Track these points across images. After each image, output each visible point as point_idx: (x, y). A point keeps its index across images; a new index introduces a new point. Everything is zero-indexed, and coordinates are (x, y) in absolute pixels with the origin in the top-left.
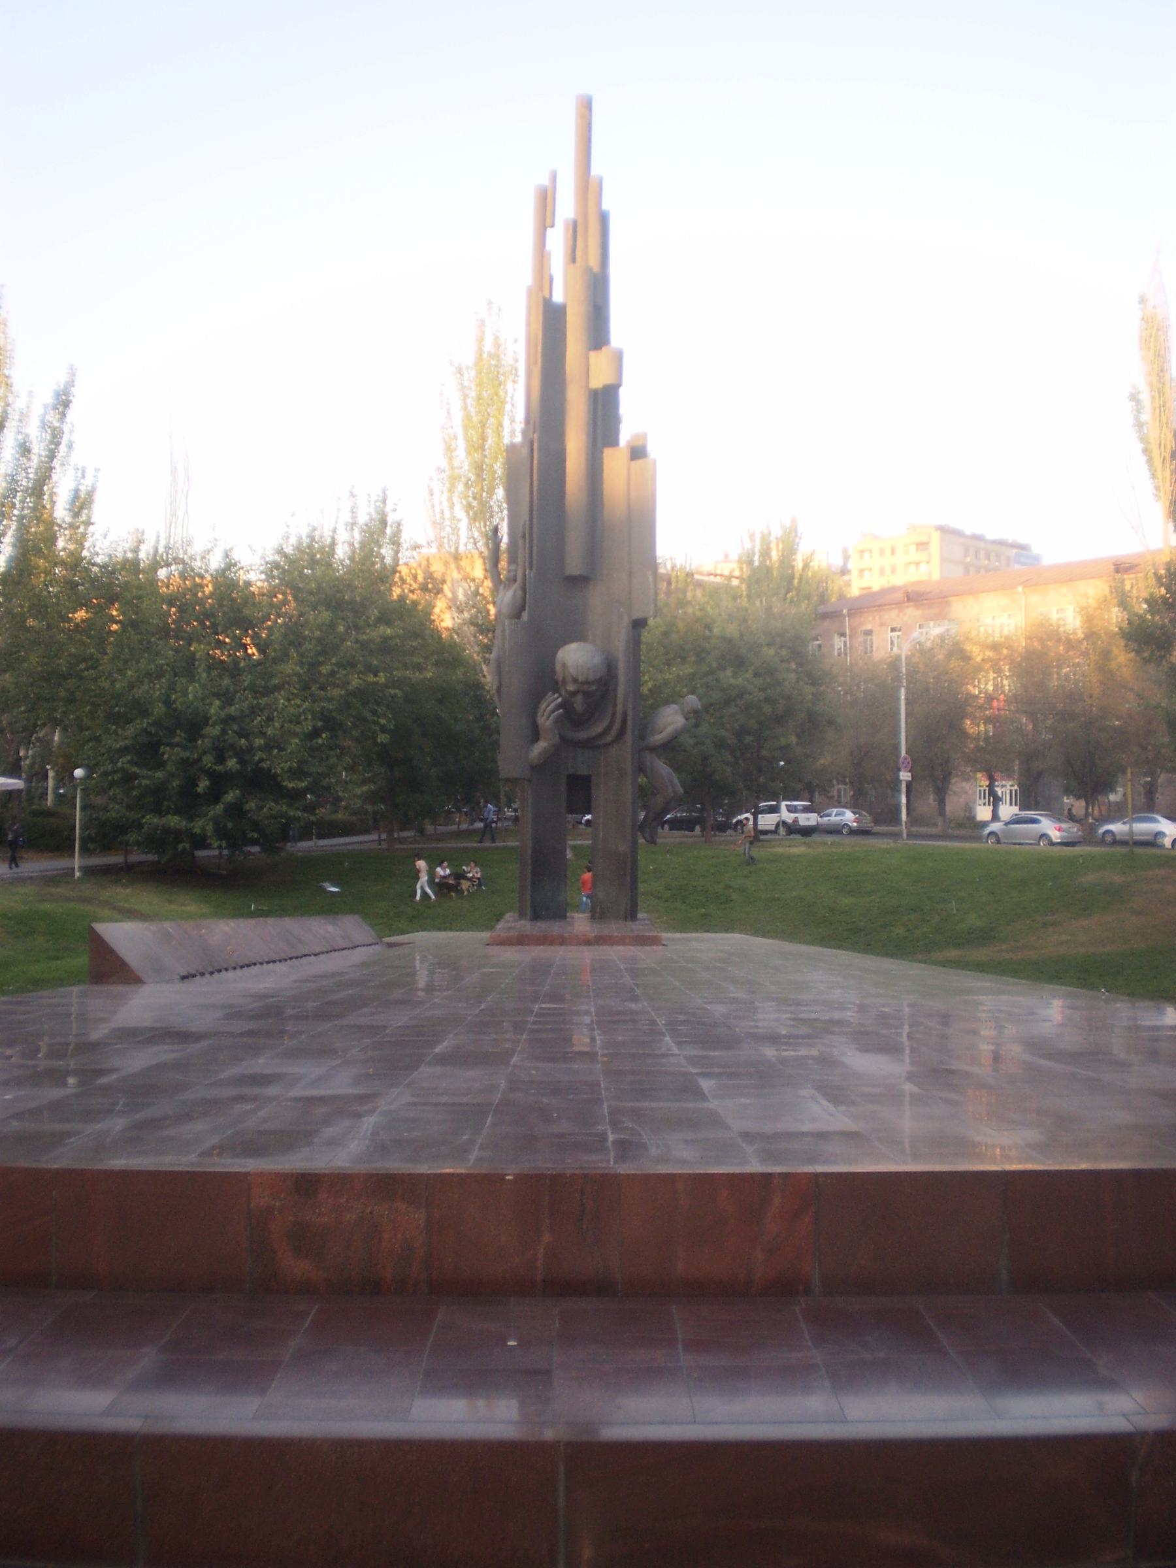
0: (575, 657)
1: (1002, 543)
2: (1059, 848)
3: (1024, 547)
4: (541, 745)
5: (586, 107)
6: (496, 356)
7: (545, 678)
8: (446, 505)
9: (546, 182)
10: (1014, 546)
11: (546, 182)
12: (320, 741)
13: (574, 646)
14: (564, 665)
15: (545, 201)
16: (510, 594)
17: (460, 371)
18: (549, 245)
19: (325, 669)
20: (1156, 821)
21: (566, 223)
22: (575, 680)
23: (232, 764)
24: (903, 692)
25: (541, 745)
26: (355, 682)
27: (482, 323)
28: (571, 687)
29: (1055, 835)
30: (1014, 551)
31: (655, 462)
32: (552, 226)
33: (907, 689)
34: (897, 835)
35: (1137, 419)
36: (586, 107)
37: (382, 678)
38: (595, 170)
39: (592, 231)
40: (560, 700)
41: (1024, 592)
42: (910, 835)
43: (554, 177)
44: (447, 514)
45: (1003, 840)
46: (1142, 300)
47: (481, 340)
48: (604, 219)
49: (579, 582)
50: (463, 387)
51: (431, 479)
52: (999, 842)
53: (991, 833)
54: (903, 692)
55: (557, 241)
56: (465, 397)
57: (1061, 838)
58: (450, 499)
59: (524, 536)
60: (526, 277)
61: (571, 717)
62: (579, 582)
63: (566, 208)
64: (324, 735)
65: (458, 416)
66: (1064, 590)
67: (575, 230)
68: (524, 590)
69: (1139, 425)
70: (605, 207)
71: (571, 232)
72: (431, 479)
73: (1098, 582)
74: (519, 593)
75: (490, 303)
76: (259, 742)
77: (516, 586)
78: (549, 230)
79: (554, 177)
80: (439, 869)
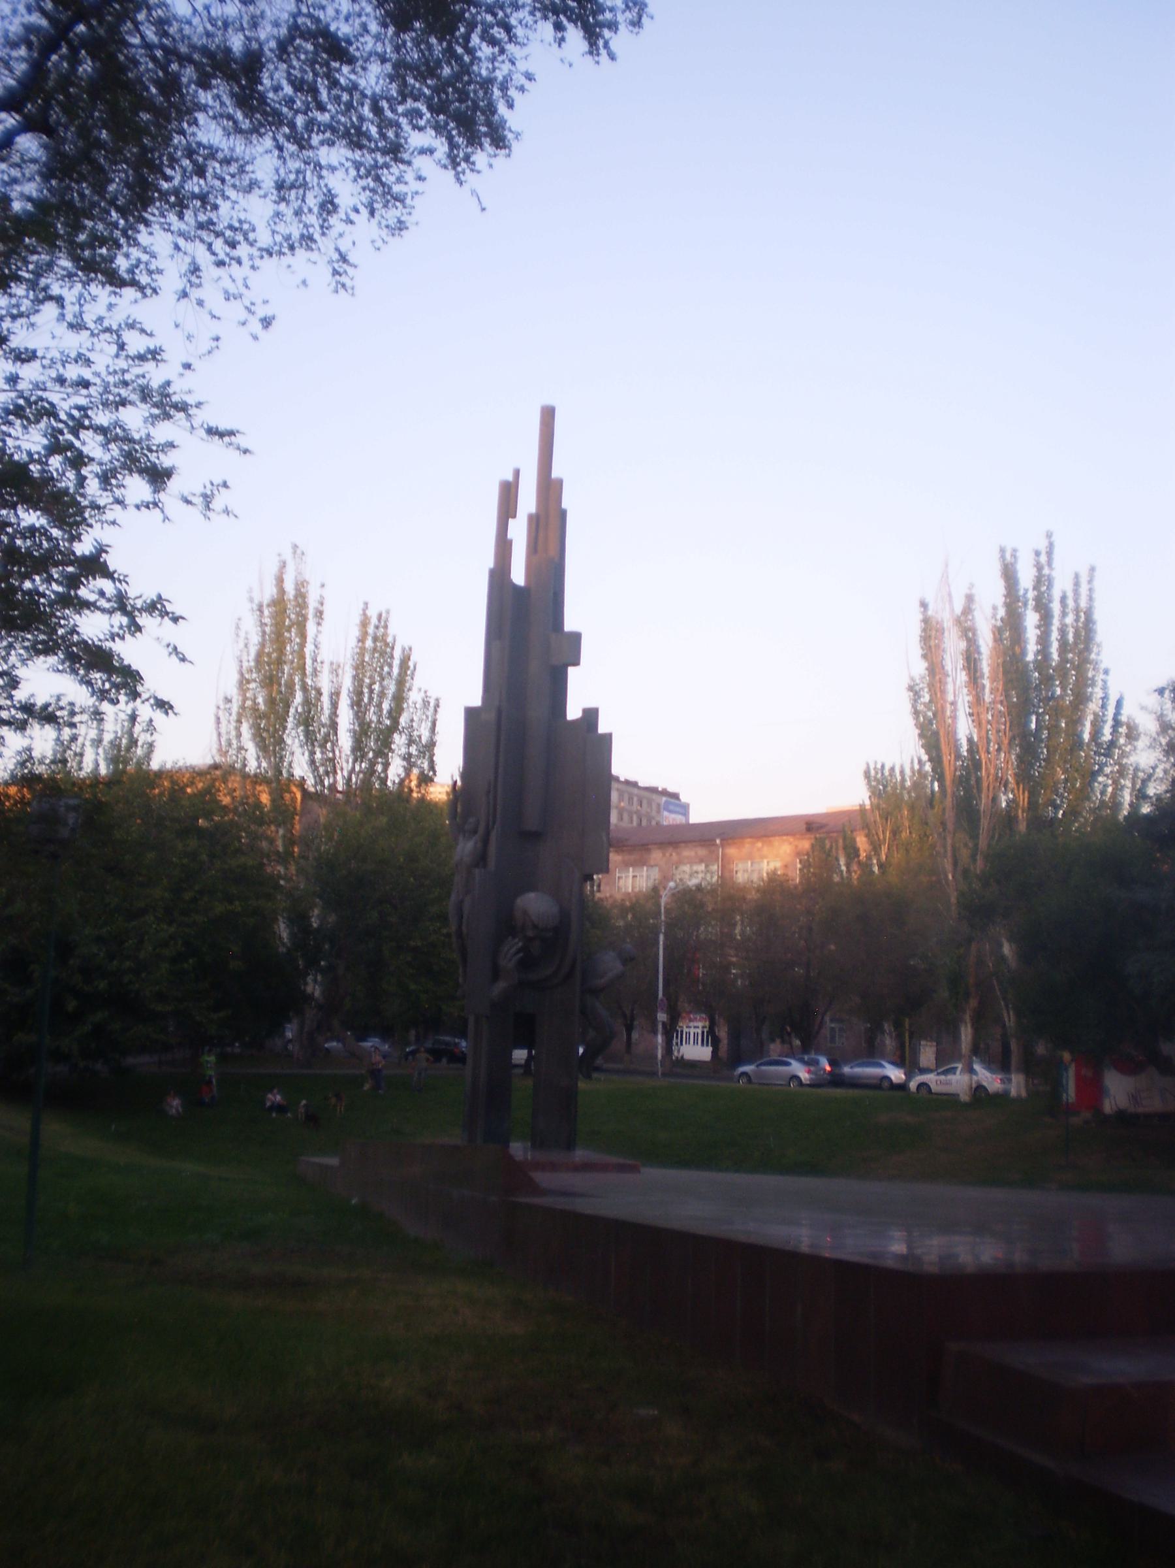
0: (535, 904)
1: (653, 790)
2: (808, 1090)
3: (675, 796)
4: (501, 985)
5: (548, 416)
6: (301, 596)
7: (508, 924)
8: (233, 733)
9: (510, 478)
10: (665, 793)
11: (510, 478)
12: (186, 966)
13: (532, 895)
14: (525, 913)
15: (508, 494)
16: (470, 845)
17: (260, 609)
18: (511, 535)
19: (188, 896)
20: (882, 1066)
21: (530, 517)
22: (535, 927)
23: (102, 985)
24: (661, 937)
25: (501, 985)
26: (219, 908)
27: (283, 565)
28: (530, 933)
29: (804, 1076)
30: (664, 799)
31: (610, 735)
32: (514, 516)
33: (666, 935)
34: (654, 1074)
35: (914, 707)
36: (548, 416)
37: (237, 906)
39: (550, 525)
40: (520, 944)
41: (722, 845)
42: (664, 1074)
43: (517, 473)
44: (234, 742)
45: (754, 1080)
46: (924, 605)
47: (280, 581)
48: (563, 514)
49: (533, 837)
50: (263, 625)
51: (218, 708)
52: (750, 1081)
53: (744, 1074)
54: (661, 937)
55: (518, 531)
56: (264, 633)
57: (811, 1079)
58: (238, 729)
59: (489, 792)
60: (488, 561)
61: (527, 962)
62: (533, 837)
63: (527, 502)
64: (191, 961)
65: (253, 650)
66: (759, 845)
67: (537, 523)
68: (486, 841)
69: (916, 713)
70: (564, 506)
71: (534, 526)
72: (218, 708)
74: (479, 845)
75: (295, 547)
76: (128, 964)
79: (517, 473)
80: (270, 1096)
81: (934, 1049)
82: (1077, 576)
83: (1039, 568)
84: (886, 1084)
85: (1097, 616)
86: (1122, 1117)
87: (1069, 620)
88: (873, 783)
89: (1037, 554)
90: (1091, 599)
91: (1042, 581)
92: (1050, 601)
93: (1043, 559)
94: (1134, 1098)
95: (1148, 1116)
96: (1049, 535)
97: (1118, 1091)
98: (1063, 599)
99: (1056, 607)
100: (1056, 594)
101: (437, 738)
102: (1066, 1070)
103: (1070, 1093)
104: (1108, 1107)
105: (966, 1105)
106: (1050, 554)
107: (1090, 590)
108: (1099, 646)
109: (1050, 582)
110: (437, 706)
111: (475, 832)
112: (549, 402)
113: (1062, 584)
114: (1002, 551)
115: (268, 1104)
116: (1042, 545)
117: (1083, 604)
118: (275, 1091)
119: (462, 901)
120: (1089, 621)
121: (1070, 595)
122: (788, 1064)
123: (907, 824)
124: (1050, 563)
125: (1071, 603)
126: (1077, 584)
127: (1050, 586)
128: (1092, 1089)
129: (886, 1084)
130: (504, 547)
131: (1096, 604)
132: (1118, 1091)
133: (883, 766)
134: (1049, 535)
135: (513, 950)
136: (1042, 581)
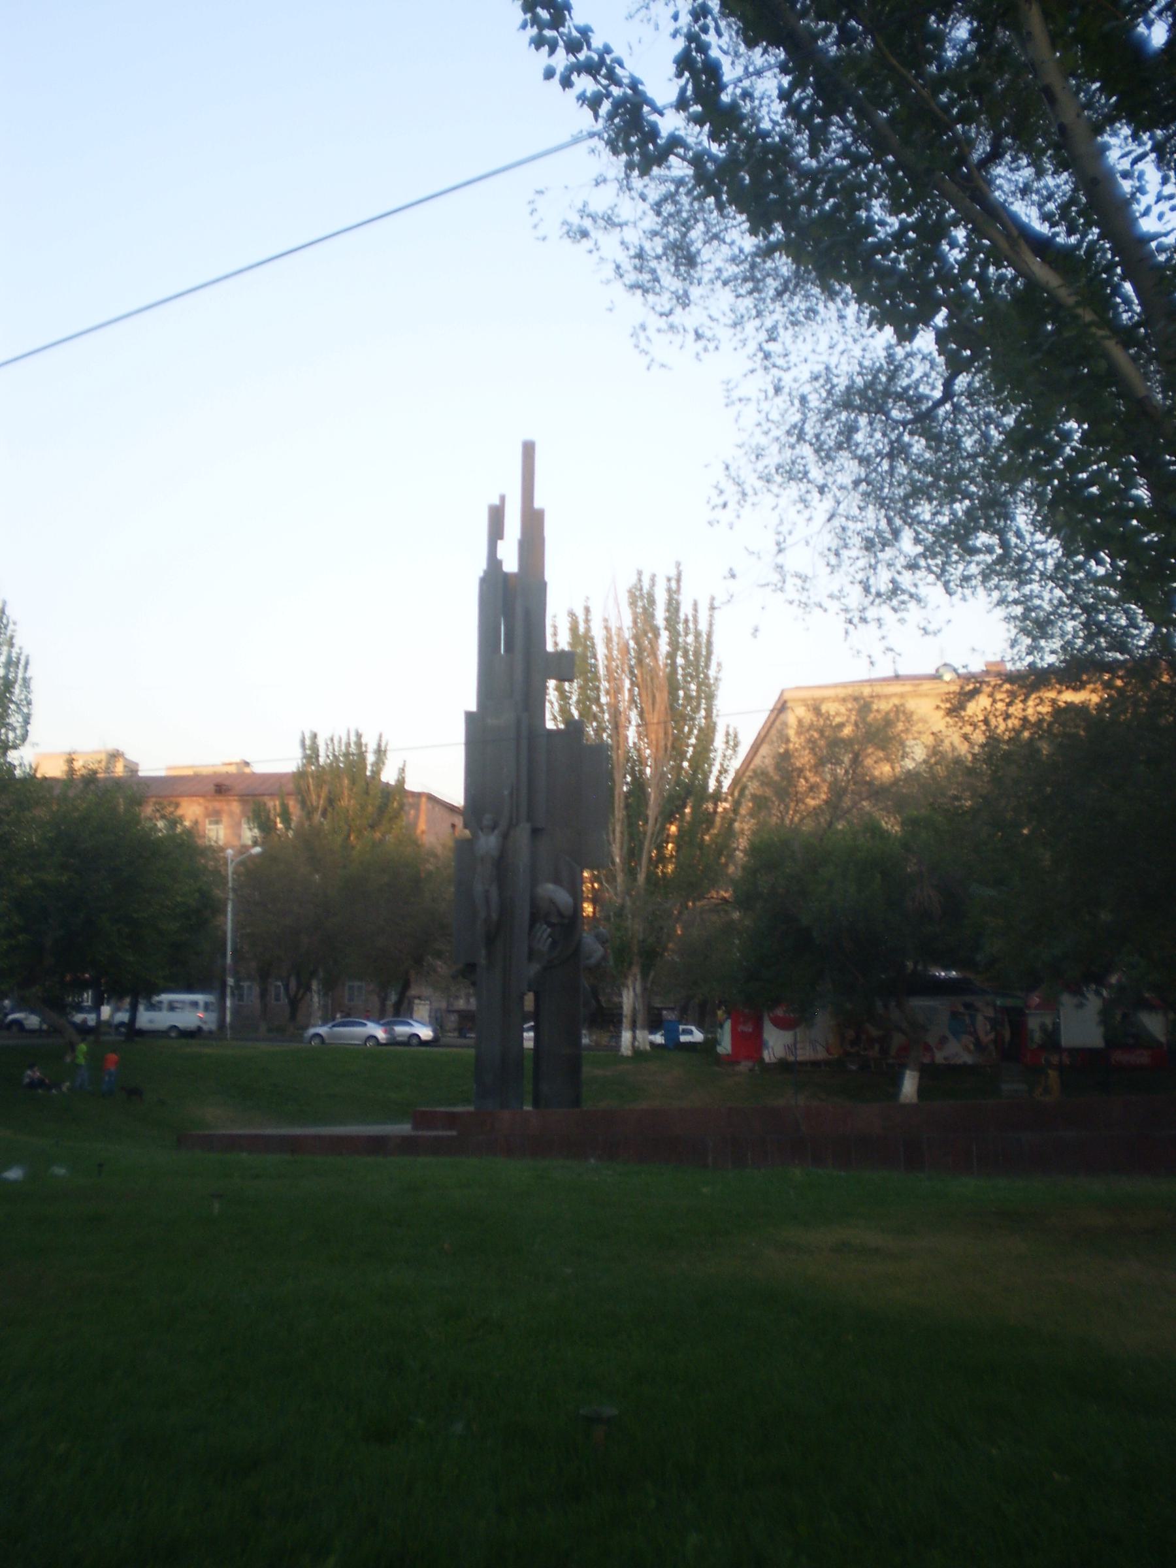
5: (529, 450)
11: (497, 502)
14: (552, 902)
15: (496, 516)
22: (560, 915)
25: (534, 968)
28: (554, 920)
36: (529, 450)
38: (538, 504)
43: (503, 499)
53: (318, 1035)
59: (511, 794)
68: (505, 836)
73: (201, 800)
77: (496, 832)
78: (500, 542)
79: (503, 499)
80: (29, 1072)
81: (427, 1007)
82: (695, 604)
83: (669, 590)
84: (415, 1041)
85: (715, 639)
86: (783, 1066)
87: (690, 639)
88: (308, 752)
89: (669, 580)
90: (711, 625)
91: (673, 607)
92: (678, 623)
93: (674, 585)
94: (792, 1048)
95: (801, 1064)
96: (678, 564)
97: (776, 1043)
98: (686, 621)
99: (681, 627)
100: (682, 616)
101: (32, 696)
102: (721, 1026)
103: (725, 1046)
104: (767, 1056)
105: (628, 1057)
106: (678, 581)
107: (711, 616)
108: (719, 665)
109: (678, 603)
110: (27, 663)
111: (493, 828)
112: (529, 437)
113: (686, 610)
114: (640, 573)
115: (27, 1080)
116: (673, 573)
117: (703, 627)
118: (36, 1069)
119: (487, 891)
120: (709, 643)
121: (690, 618)
122: (365, 1025)
123: (346, 792)
124: (678, 591)
125: (691, 625)
126: (696, 610)
127: (677, 610)
128: (750, 1043)
129: (415, 1041)
130: (494, 562)
131: (714, 627)
132: (776, 1043)
133: (315, 736)
134: (678, 564)
135: (545, 936)
136: (673, 607)
